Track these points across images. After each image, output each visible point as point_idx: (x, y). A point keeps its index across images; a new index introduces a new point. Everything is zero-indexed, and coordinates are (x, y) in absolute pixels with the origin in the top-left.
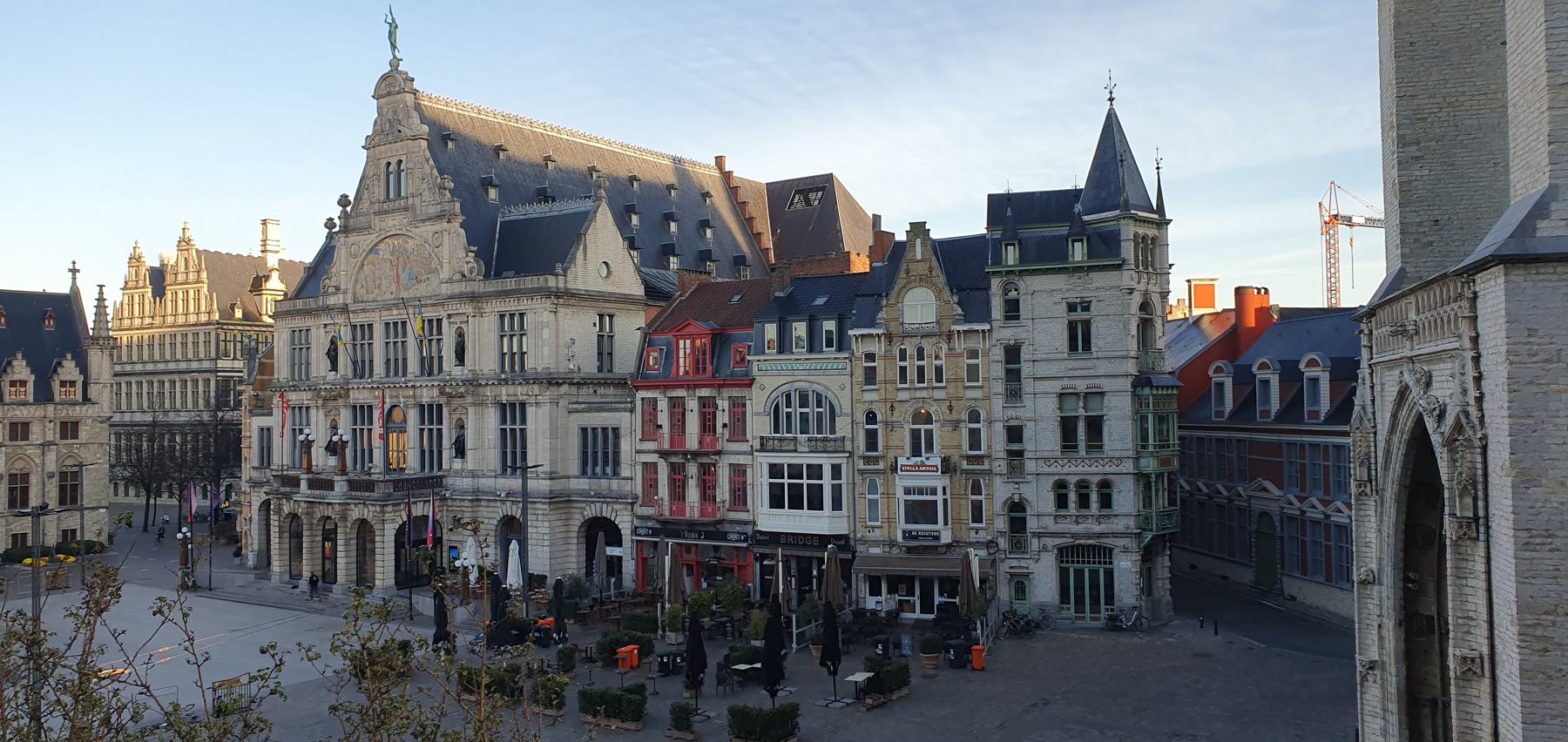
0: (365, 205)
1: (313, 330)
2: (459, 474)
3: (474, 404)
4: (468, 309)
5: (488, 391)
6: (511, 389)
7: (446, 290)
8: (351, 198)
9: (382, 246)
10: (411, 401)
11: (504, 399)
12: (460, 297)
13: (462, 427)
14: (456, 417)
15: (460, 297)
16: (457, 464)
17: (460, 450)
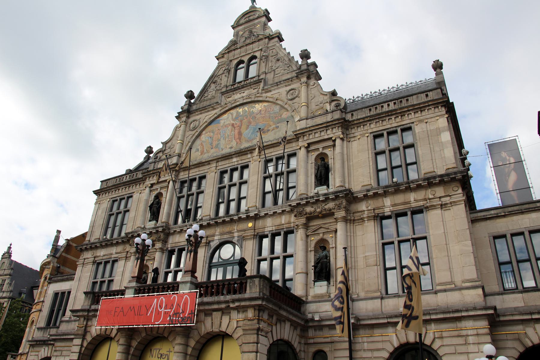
0: (212, 92)
1: (135, 196)
2: (320, 299)
3: (346, 220)
4: (337, 132)
5: (363, 206)
6: (400, 198)
7: (303, 124)
8: (196, 95)
9: (225, 116)
10: (251, 232)
11: (387, 211)
12: (327, 126)
13: (324, 248)
14: (314, 239)
15: (327, 126)
16: (321, 288)
17: (323, 271)
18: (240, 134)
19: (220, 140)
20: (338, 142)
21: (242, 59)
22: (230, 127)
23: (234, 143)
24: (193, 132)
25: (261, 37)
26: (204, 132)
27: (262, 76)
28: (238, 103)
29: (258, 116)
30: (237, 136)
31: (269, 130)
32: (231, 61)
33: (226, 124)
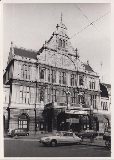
18: (62, 62)
19: (57, 62)
20: (85, 77)
21: (61, 39)
22: (60, 59)
23: (61, 65)
24: (50, 55)
25: (66, 36)
26: (52, 57)
27: (68, 49)
28: (62, 53)
29: (66, 60)
30: (62, 63)
31: (69, 66)
32: (58, 38)
33: (58, 57)
